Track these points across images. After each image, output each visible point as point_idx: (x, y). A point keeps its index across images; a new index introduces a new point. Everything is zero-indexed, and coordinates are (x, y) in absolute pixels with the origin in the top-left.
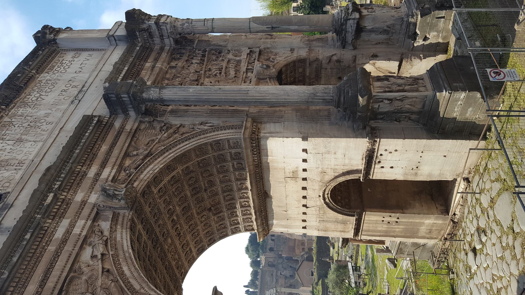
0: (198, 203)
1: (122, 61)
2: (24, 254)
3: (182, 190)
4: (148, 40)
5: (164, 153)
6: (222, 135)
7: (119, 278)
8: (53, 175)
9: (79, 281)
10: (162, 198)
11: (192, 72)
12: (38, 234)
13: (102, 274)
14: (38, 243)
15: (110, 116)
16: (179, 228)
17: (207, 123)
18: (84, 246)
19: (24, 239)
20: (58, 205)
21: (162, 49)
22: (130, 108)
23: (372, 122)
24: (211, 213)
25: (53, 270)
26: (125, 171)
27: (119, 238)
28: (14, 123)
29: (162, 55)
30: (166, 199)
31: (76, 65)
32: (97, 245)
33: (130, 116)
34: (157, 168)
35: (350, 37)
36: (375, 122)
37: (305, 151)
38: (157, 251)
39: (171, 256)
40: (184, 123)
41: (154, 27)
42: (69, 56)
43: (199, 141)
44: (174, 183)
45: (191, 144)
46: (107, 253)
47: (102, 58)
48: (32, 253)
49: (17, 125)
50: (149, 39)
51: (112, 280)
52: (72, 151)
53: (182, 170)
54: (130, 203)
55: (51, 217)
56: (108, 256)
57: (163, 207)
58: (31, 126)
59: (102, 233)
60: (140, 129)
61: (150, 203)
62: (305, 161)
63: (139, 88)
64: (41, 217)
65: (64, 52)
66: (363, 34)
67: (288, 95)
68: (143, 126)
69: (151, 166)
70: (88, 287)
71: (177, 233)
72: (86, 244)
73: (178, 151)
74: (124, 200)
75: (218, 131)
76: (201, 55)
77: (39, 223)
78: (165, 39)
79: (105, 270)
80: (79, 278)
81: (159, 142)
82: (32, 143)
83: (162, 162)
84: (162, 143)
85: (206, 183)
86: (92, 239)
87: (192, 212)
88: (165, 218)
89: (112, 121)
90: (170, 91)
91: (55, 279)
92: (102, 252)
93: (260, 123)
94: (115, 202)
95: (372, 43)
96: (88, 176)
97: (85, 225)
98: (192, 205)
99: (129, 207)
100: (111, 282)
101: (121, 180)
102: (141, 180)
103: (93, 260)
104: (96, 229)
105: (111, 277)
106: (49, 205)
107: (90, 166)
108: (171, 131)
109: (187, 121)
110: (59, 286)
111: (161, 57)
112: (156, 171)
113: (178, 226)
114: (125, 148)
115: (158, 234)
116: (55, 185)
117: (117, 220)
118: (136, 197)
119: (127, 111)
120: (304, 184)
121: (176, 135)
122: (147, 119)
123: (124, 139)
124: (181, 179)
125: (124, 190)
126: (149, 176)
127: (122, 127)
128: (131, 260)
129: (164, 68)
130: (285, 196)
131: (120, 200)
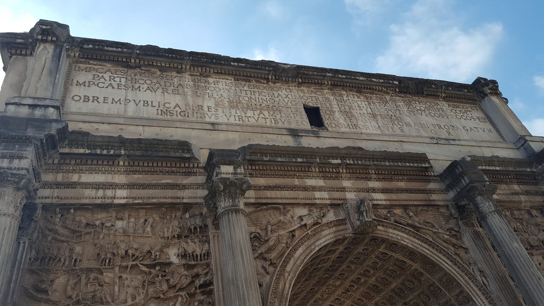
0: (388, 299)
1: (503, 161)
2: (285, 164)
5: (426, 243)
7: (291, 248)
8: (356, 154)
9: (278, 215)
10: (377, 259)
11: (539, 237)
12: (304, 166)
13: (289, 232)
14: (297, 170)
15: (437, 176)
16: (354, 289)
17: (485, 278)
18: (307, 206)
19: (296, 158)
20: (333, 170)
25: (280, 191)
26: (389, 212)
27: (324, 233)
28: (387, 105)
29: (537, 196)
30: (377, 263)
31: (470, 124)
32: (312, 217)
33: (447, 194)
34: (406, 242)
38: (324, 274)
39: (324, 290)
42: (477, 114)
44: (398, 266)
46: (308, 228)
47: (494, 142)
48: (288, 169)
49: (387, 108)
51: (287, 242)
52: (385, 159)
53: (416, 269)
54: (360, 230)
55: (321, 170)
56: (305, 230)
57: (369, 264)
58: (391, 118)
59: (323, 216)
60: (438, 209)
61: (367, 249)
63: (484, 190)
64: (318, 162)
65: (478, 108)
68: (443, 210)
69: (405, 235)
70: (276, 225)
71: (348, 289)
72: (309, 207)
73: (435, 257)
74: (361, 223)
75: (483, 294)
77: (313, 163)
79: (293, 233)
80: (280, 214)
81: (435, 233)
82: (377, 126)
83: (415, 245)
84: (435, 237)
85: (413, 301)
86: (315, 210)
88: (358, 270)
89: (433, 180)
90: (500, 222)
91: (274, 196)
94: (355, 216)
96: (369, 182)
97: (325, 199)
98: (383, 293)
99: (356, 230)
100: (285, 242)
101: (377, 213)
102: (386, 232)
103: (298, 219)
104: (325, 210)
105: (289, 241)
106: (330, 164)
107: (378, 180)
108: (454, 241)
109: (475, 254)
110: (269, 201)
111: (534, 196)
112: (402, 242)
113: (356, 287)
115: (341, 269)
116: (349, 160)
117: (340, 224)
118: (368, 233)
119: (452, 189)
121: (452, 248)
122: (453, 211)
123: (420, 198)
124: (406, 272)
125: (370, 220)
126: (395, 238)
127: (431, 192)
128: (309, 253)
129: (523, 204)
131: (359, 219)
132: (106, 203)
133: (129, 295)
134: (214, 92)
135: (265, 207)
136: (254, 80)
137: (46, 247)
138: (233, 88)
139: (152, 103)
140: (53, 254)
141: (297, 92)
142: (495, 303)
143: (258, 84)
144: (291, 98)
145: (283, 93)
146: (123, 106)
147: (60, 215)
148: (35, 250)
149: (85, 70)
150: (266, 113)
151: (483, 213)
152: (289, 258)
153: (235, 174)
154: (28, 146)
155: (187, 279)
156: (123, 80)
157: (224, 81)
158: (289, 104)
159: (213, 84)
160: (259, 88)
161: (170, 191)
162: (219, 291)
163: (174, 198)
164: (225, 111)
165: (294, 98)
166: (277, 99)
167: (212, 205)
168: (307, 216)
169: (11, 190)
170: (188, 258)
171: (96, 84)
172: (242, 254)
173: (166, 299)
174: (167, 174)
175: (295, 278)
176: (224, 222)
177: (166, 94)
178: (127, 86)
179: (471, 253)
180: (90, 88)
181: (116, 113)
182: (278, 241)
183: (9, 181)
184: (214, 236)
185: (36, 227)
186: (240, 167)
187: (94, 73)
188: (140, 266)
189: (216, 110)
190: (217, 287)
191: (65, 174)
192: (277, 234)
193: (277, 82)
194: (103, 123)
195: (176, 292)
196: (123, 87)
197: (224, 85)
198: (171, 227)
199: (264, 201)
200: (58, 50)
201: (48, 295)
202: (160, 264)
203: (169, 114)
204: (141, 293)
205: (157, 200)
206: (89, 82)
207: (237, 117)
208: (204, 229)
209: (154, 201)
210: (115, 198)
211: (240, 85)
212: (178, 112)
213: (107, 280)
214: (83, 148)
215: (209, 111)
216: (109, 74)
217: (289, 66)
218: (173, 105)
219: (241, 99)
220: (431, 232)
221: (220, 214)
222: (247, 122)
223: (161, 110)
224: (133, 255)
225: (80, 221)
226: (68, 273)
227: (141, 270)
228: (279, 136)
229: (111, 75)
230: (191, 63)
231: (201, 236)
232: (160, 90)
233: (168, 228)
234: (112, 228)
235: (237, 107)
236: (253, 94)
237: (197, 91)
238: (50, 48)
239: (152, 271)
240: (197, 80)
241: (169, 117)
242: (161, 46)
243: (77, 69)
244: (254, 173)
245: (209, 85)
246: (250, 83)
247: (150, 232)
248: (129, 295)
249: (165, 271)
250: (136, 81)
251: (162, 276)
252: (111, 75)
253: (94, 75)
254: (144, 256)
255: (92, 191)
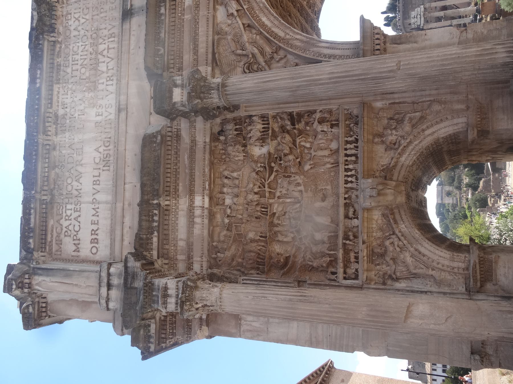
32: (229, 3)
51: (255, 33)
56: (243, 11)
72: (218, 4)
79: (246, 26)
91: (204, 45)
92: (236, 8)
100: (255, 35)
110: (210, 50)
128: (267, 10)
132: (208, 214)
133: (295, 189)
134: (77, 108)
135: (217, 56)
136: (58, 60)
137: (248, 262)
138: (70, 86)
139: (96, 176)
140: (254, 256)
141: (71, 6)
143: (63, 55)
144: (79, 14)
145: (72, 24)
146: (100, 206)
147: (219, 254)
148: (249, 271)
149: (60, 246)
150: (102, 47)
152: (272, 33)
153: (182, 86)
154: (153, 284)
155: (285, 137)
156: (69, 207)
157: (61, 97)
158: (87, 17)
159: (66, 109)
160: (68, 54)
161: (197, 156)
162: (298, 107)
163: (205, 151)
164: (101, 97)
165: (79, 10)
166: (82, 32)
167: (215, 112)
168: (228, 8)
169: (197, 292)
170: (265, 136)
171: (76, 233)
172: (268, 81)
173: (302, 156)
174: (178, 159)
175: (292, 27)
176: (234, 99)
177: (83, 162)
178: (76, 202)
180: (81, 239)
181: (109, 212)
182: (254, 43)
183: (189, 295)
184: (246, 111)
185: (229, 273)
186: (174, 80)
187: (62, 236)
188: (269, 180)
189: (100, 106)
190: (295, 109)
191: (178, 253)
192: (247, 44)
193: (58, 31)
194: (123, 223)
195: (296, 147)
196: (78, 207)
197: (66, 96)
198: (234, 154)
199: (210, 56)
200: (40, 272)
201: (289, 256)
202: (269, 163)
203: (107, 159)
204: (295, 178)
205: (206, 167)
206: (74, 240)
207: (108, 83)
208: (238, 121)
209: (207, 170)
210: (204, 207)
211: (66, 78)
212: (105, 148)
213: (280, 209)
214: (152, 238)
215: (102, 115)
216: (63, 222)
217: (35, 13)
218: (97, 155)
219: (84, 77)
221: (225, 103)
222: (114, 71)
223: (104, 166)
224: (260, 187)
225: (225, 236)
226: (271, 242)
227: (274, 179)
228: (132, 33)
229: (64, 219)
230: (42, 134)
231: (244, 124)
232: (79, 169)
233: (234, 156)
234: (232, 208)
235: (95, 82)
236: (76, 62)
237: (76, 128)
238: (37, 279)
239: (275, 170)
240: (64, 128)
241: (112, 158)
242: (22, 169)
243: (59, 253)
244: (177, 65)
245: (69, 115)
246: (62, 65)
247: (239, 173)
248: (295, 189)
249: (276, 158)
250: (69, 193)
251: (281, 160)
252: (64, 219)
253: (65, 236)
254: (261, 177)
255: (195, 228)
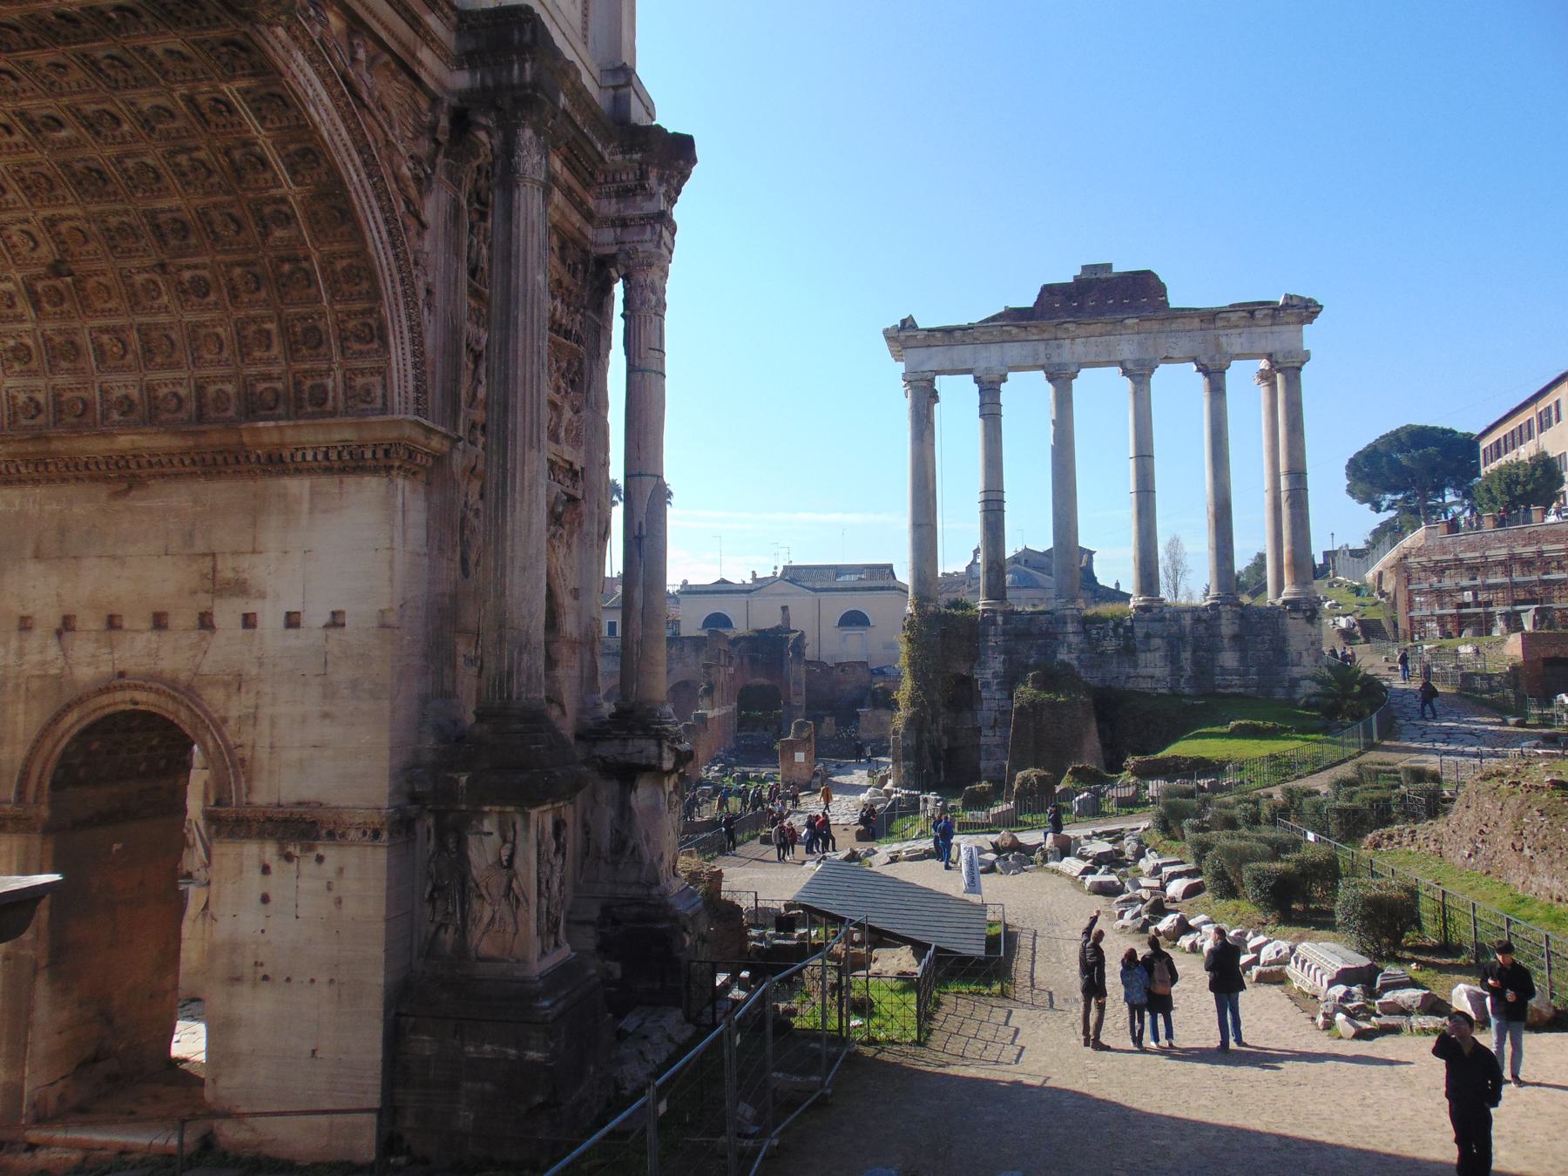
0: (108, 230)
3: (188, 184)
4: (614, 181)
5: (360, 152)
6: (400, 355)
21: (589, 216)
22: (483, 79)
23: (431, 821)
24: (42, 270)
29: (576, 212)
34: (319, 114)
35: (608, 750)
36: (429, 831)
37: (336, 621)
40: (428, 235)
41: (649, 207)
43: (387, 273)
44: (232, 162)
45: (380, 246)
50: (615, 185)
53: (283, 200)
62: (292, 621)
63: (549, 124)
66: (615, 786)
67: (524, 569)
68: (424, 104)
75: (413, 341)
76: (569, 328)
78: (615, 232)
81: (388, 143)
83: (336, 138)
87: (70, 200)
90: (539, 215)
93: (427, 479)
95: (588, 812)
108: (413, 192)
109: (432, 246)
111: (572, 208)
112: (312, 110)
114: (376, 26)
119: (473, 68)
120: (182, 619)
122: (444, 122)
124: (244, 190)
126: (300, 84)
127: (427, 37)
130: (119, 552)
142: (424, 372)
151: (516, 171)
179: (427, 243)
220: (383, 136)
